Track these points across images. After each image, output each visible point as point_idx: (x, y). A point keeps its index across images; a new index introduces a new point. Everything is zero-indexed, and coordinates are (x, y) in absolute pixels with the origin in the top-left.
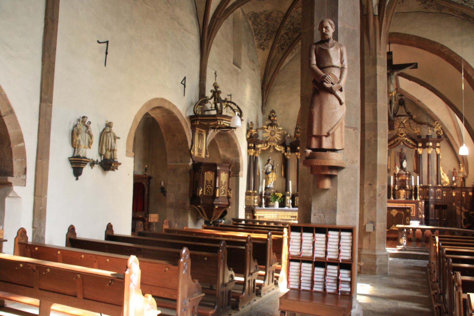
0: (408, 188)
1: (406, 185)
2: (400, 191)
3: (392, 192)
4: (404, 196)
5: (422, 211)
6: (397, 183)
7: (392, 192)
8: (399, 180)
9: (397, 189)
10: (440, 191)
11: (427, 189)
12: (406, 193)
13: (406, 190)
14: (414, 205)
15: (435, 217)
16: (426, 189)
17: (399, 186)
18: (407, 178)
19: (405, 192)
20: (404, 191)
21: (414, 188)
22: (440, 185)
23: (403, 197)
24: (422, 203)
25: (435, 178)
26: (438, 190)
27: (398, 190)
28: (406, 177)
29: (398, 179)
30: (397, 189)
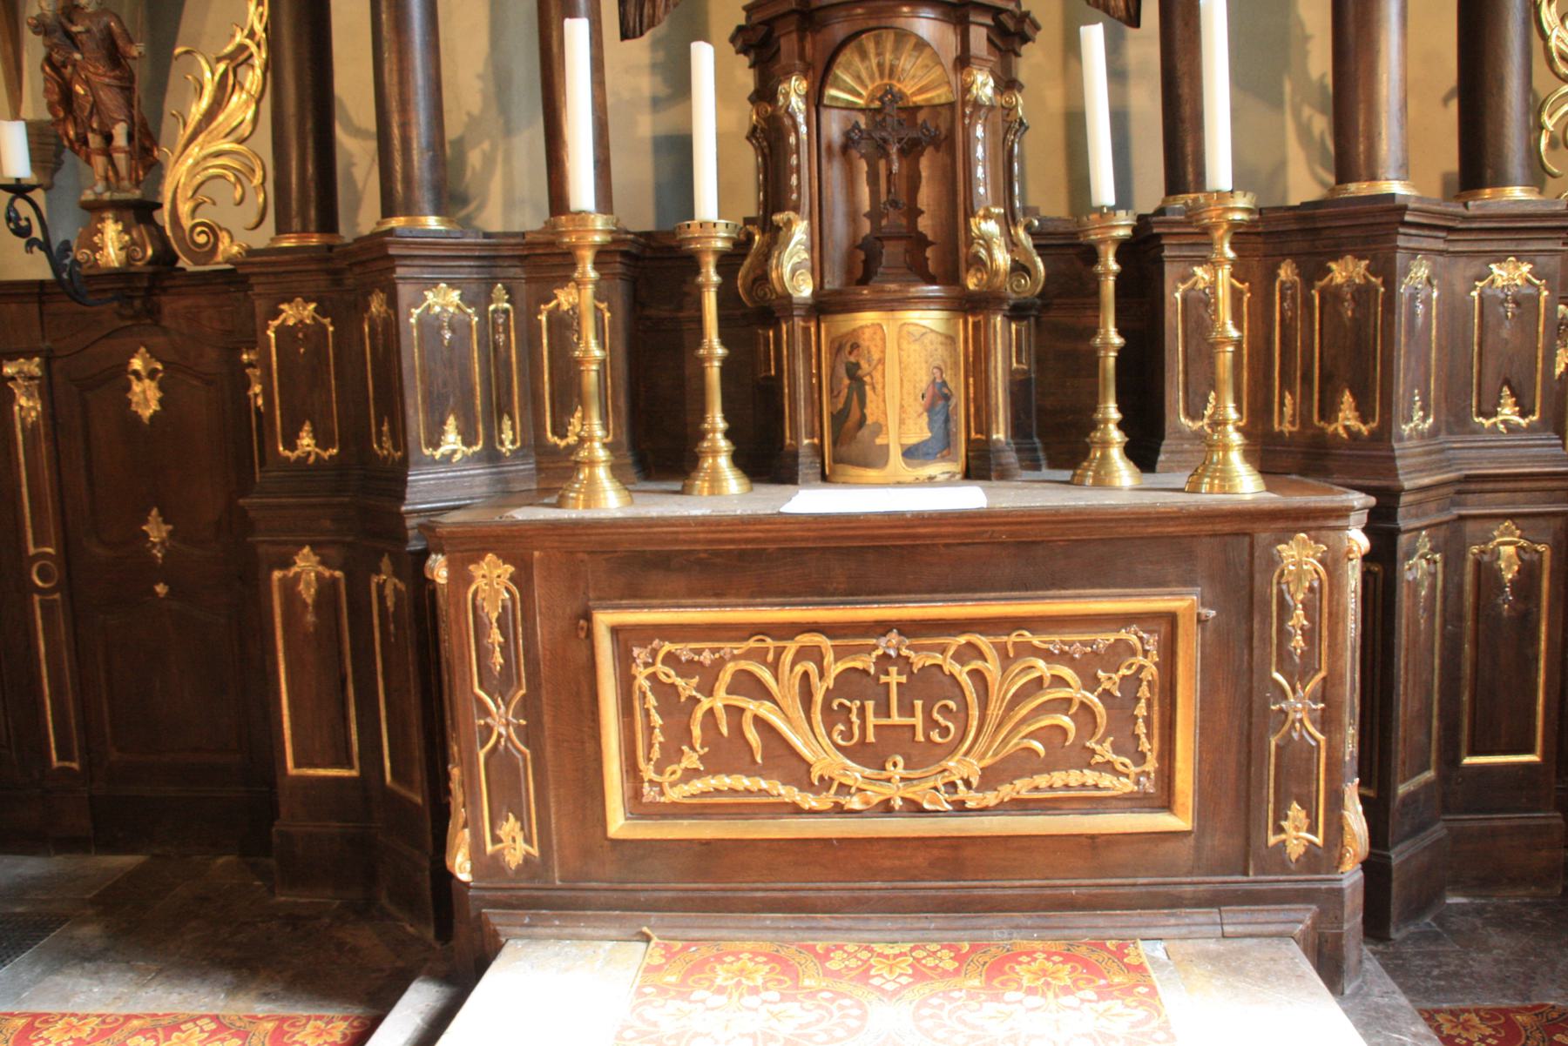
0: (1002, 259)
1: (958, 205)
2: (868, 318)
3: (714, 348)
4: (938, 399)
5: (1327, 722)
6: (800, 182)
7: (714, 348)
8: (834, 127)
9: (804, 289)
10: (1525, 302)
11: (1345, 272)
12: (977, 365)
13: (966, 305)
14: (1183, 602)
15: (1450, 759)
16: (1313, 271)
17: (839, 229)
18: (983, 85)
19: (950, 339)
20: (928, 320)
21: (1125, 250)
22: (1517, 193)
23: (918, 431)
24: (1332, 563)
25: (1304, 132)
26: (1509, 275)
27: (822, 306)
28: (964, 61)
29: (816, 100)
30: (804, 289)
